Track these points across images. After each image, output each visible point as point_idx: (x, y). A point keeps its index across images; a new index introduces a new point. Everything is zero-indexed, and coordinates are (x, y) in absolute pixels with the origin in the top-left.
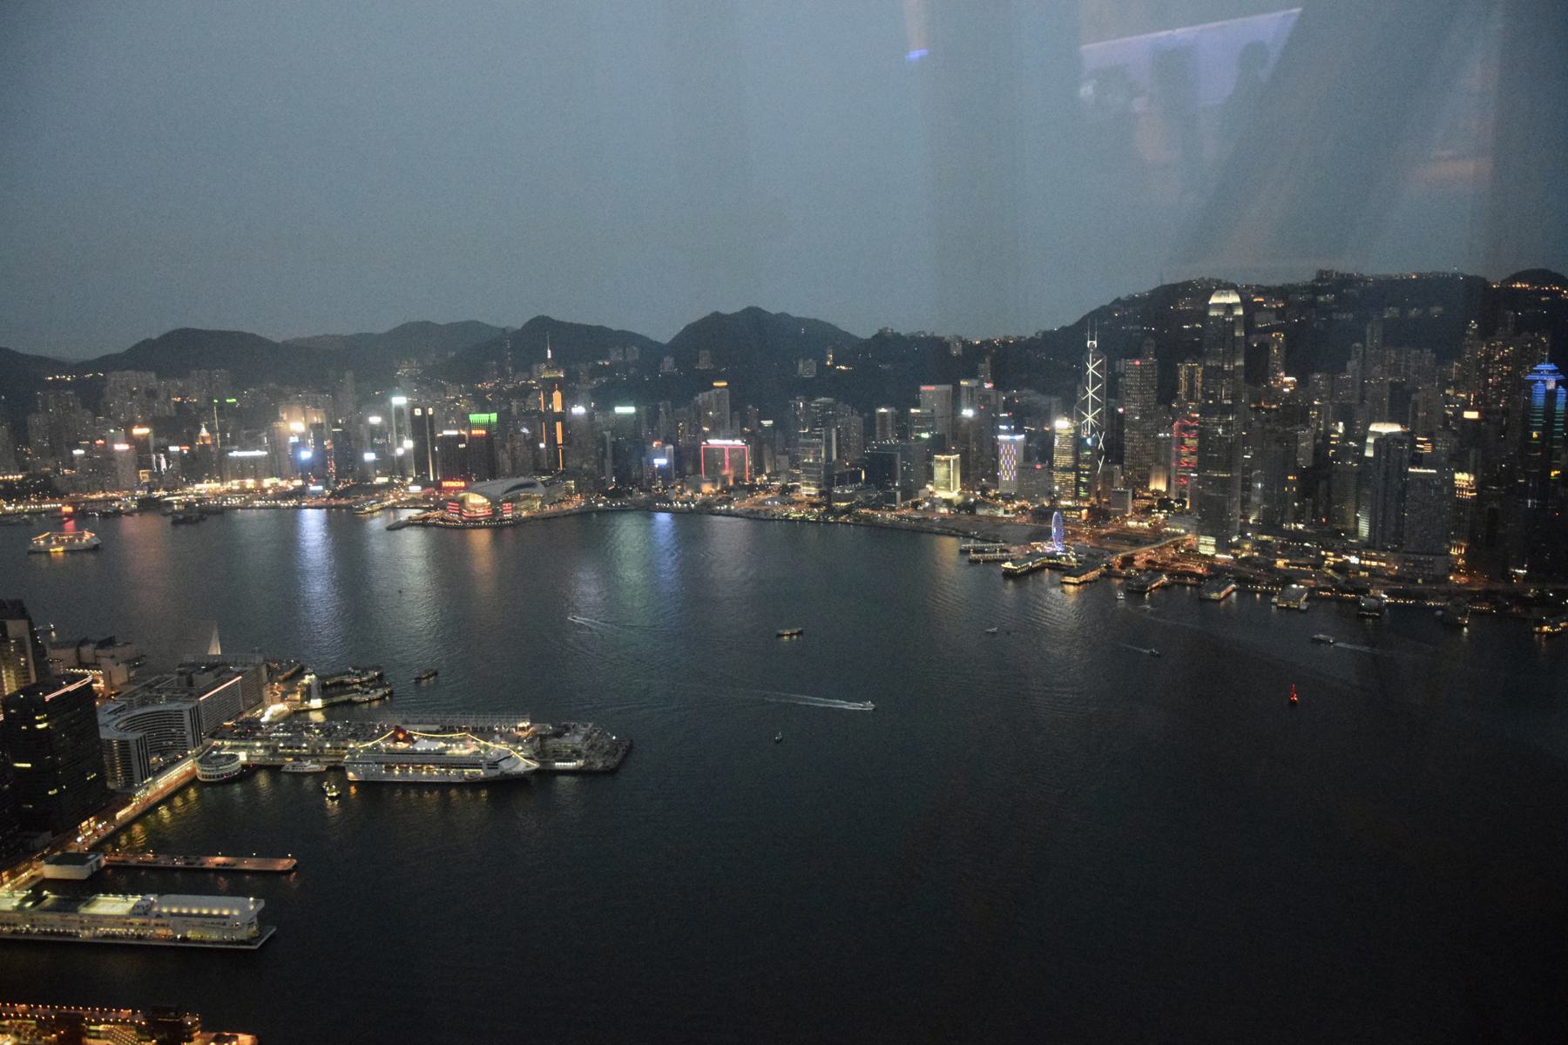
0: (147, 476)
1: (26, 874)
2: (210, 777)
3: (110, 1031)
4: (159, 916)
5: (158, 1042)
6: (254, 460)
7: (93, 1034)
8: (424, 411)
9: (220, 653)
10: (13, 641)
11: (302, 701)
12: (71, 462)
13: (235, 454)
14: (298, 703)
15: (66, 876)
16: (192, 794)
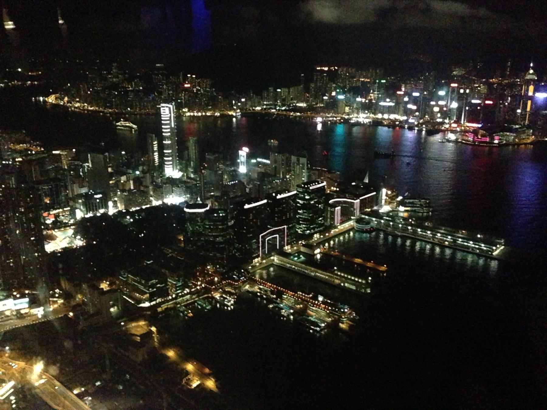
0: (348, 109)
1: (295, 248)
2: (359, 228)
3: (316, 311)
4: (337, 275)
5: (332, 320)
6: (390, 107)
7: (311, 310)
8: (465, 91)
9: (367, 181)
10: (301, 165)
11: (396, 207)
12: (322, 101)
13: (382, 103)
14: (395, 207)
15: (308, 252)
16: (352, 234)
